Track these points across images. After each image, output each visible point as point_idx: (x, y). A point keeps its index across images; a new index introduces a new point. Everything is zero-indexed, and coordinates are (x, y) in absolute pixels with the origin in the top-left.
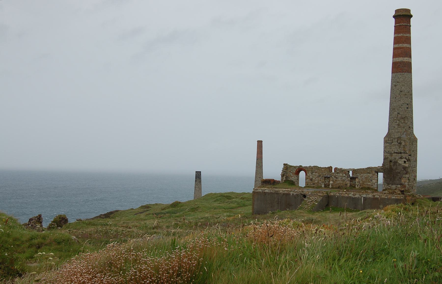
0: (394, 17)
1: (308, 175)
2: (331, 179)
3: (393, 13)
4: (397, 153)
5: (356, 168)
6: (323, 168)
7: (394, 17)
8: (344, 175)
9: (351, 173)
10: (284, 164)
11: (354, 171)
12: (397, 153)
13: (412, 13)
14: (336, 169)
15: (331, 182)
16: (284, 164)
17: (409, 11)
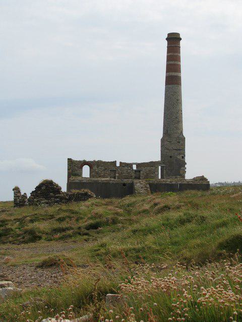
0: (167, 39)
1: (94, 168)
2: (117, 172)
3: (166, 36)
4: (176, 150)
5: (140, 162)
6: (108, 162)
7: (167, 39)
8: (129, 168)
9: (135, 167)
10: (68, 159)
11: (138, 165)
12: (176, 150)
13: (181, 37)
14: (121, 163)
15: (117, 175)
16: (68, 159)
17: (178, 34)
